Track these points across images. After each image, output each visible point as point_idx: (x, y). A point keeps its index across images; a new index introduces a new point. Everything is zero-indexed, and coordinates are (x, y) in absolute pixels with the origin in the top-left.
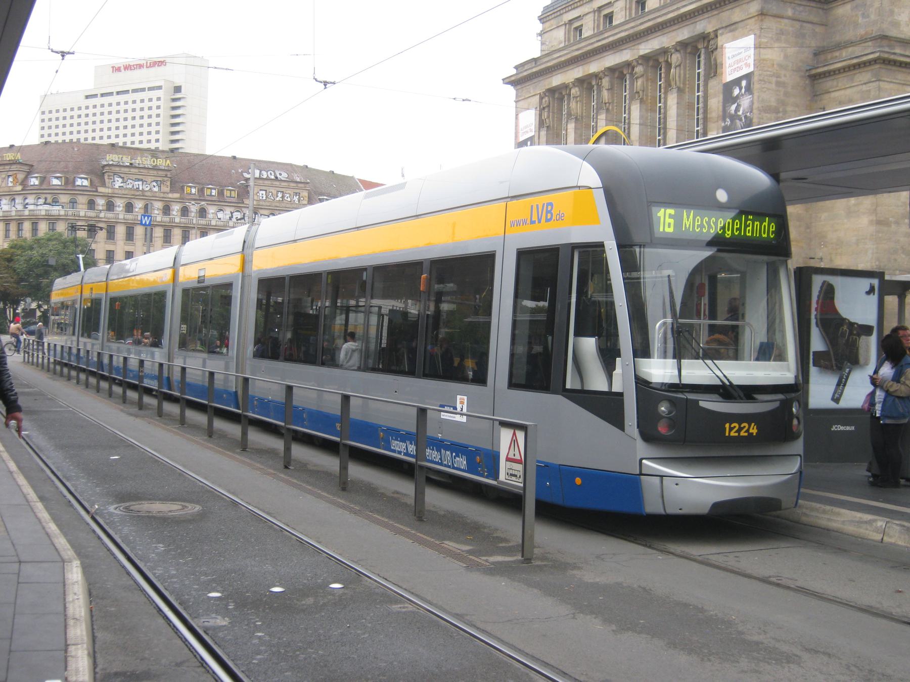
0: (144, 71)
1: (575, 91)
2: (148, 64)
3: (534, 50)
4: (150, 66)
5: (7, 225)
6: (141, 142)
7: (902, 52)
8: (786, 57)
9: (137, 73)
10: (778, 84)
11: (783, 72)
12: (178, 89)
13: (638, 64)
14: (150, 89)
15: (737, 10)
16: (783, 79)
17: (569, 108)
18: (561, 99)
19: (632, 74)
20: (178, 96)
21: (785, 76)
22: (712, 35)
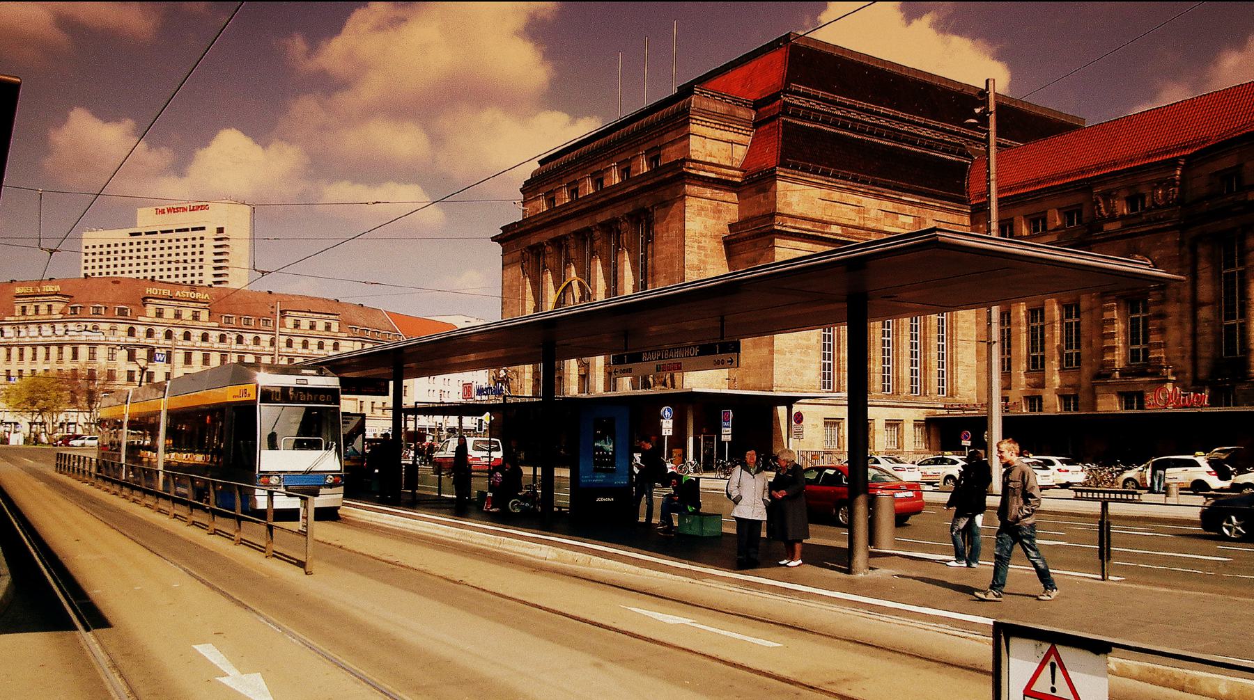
0: (188, 213)
1: (549, 249)
2: (192, 208)
3: (515, 215)
4: (193, 210)
5: (9, 350)
6: (169, 277)
7: (793, 225)
8: (706, 227)
9: (181, 215)
10: (699, 248)
11: (703, 239)
12: (220, 230)
13: (597, 230)
14: (193, 229)
15: (668, 192)
16: (703, 244)
17: (544, 262)
18: (538, 255)
19: (591, 238)
20: (220, 236)
21: (705, 241)
22: (651, 210)
